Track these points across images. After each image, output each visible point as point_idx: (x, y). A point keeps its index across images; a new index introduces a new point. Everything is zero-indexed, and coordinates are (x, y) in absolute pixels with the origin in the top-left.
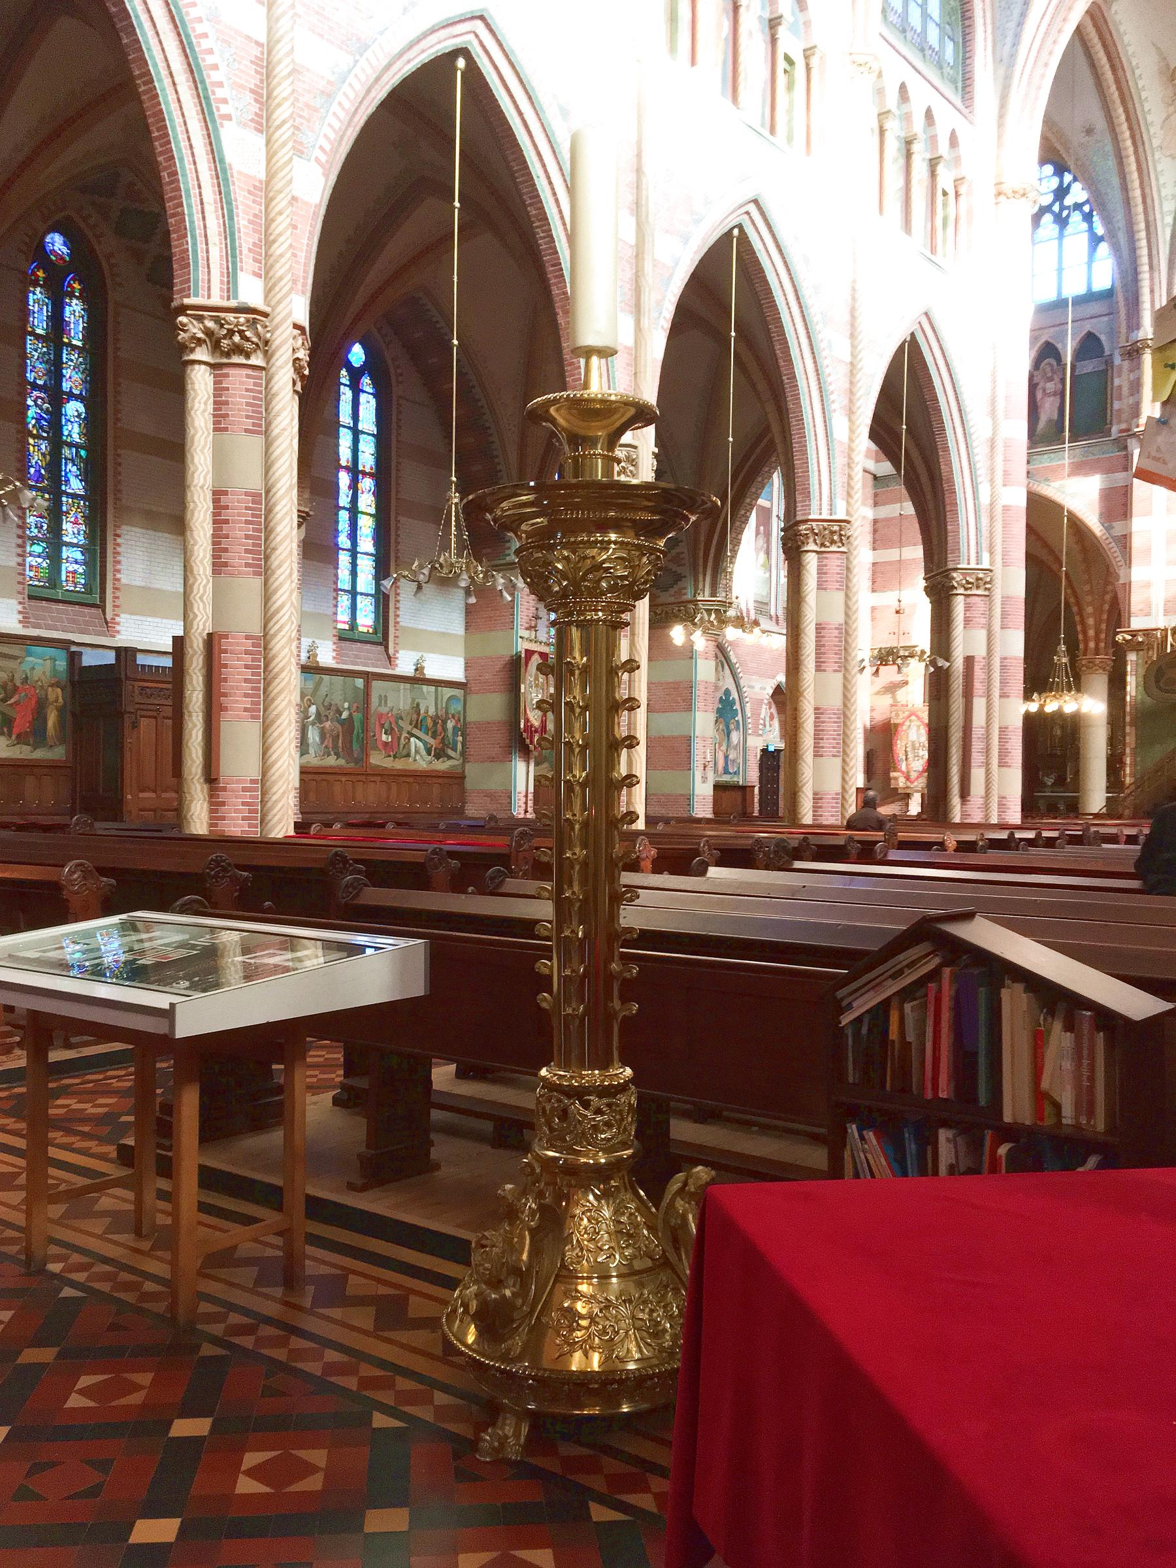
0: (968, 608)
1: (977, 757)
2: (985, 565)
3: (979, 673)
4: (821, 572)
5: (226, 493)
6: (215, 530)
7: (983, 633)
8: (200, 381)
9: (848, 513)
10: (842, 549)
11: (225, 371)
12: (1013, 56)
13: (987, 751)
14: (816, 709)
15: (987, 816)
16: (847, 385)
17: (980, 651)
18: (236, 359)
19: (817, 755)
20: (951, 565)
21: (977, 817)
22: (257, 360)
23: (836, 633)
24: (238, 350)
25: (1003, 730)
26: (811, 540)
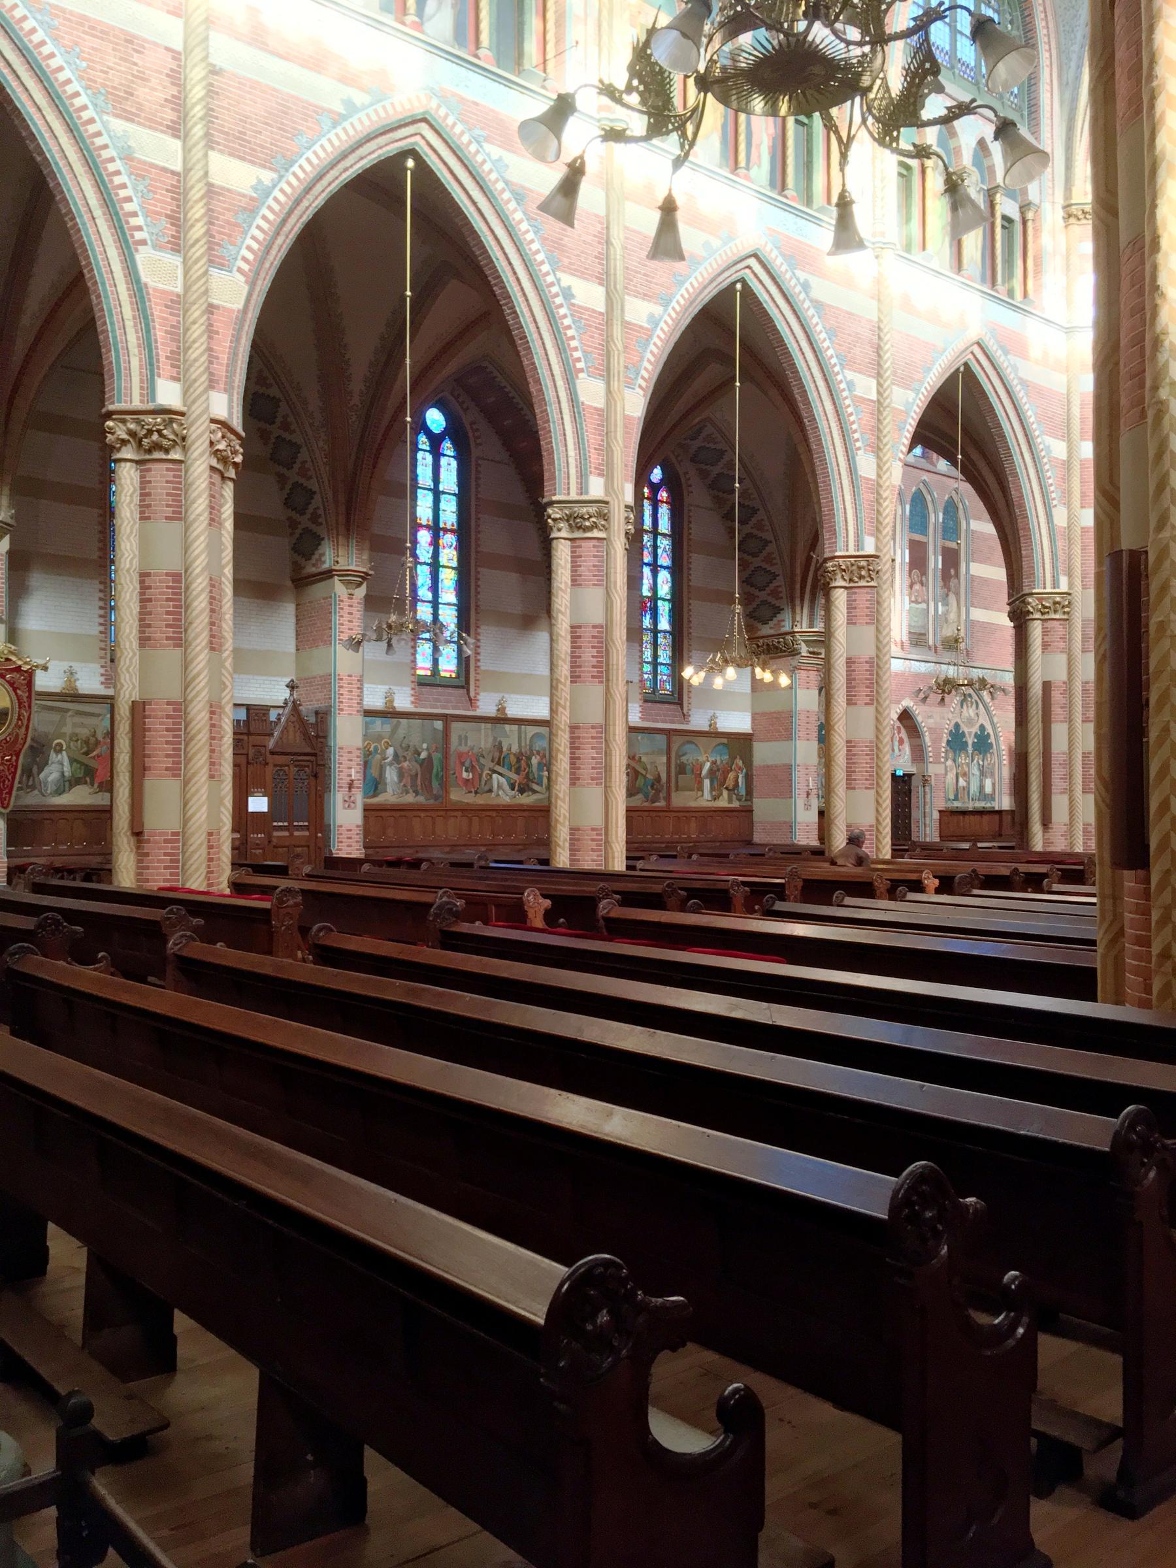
0: (1045, 632)
1: (1057, 784)
2: (1064, 588)
3: (1057, 697)
4: (851, 607)
5: (149, 575)
6: (141, 607)
7: (1063, 658)
8: (127, 478)
9: (877, 548)
10: (872, 584)
11: (148, 466)
14: (848, 742)
15: (1072, 845)
16: (873, 422)
17: (1059, 675)
18: (157, 455)
19: (850, 787)
20: (1026, 590)
21: (1059, 845)
22: (176, 455)
23: (867, 667)
24: (156, 447)
26: (839, 576)
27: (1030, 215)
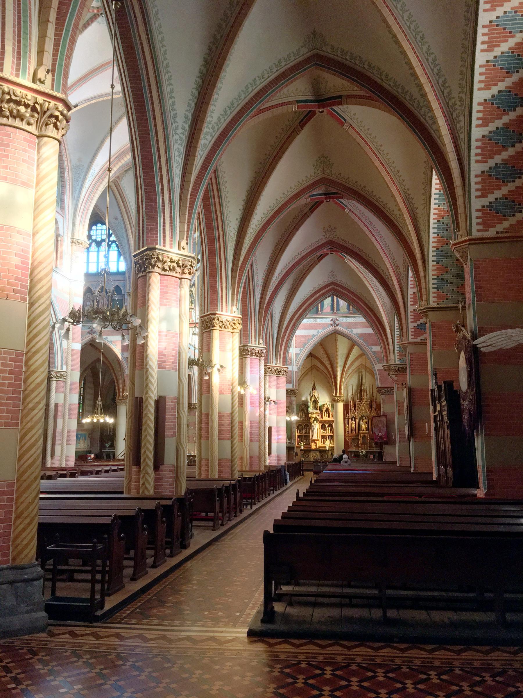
0: (57, 385)
1: (58, 441)
2: (64, 370)
3: (60, 409)
7: (63, 395)
12: (79, 198)
13: (62, 439)
15: (61, 464)
17: (61, 401)
21: (57, 464)
25: (69, 431)
27: (59, 239)
